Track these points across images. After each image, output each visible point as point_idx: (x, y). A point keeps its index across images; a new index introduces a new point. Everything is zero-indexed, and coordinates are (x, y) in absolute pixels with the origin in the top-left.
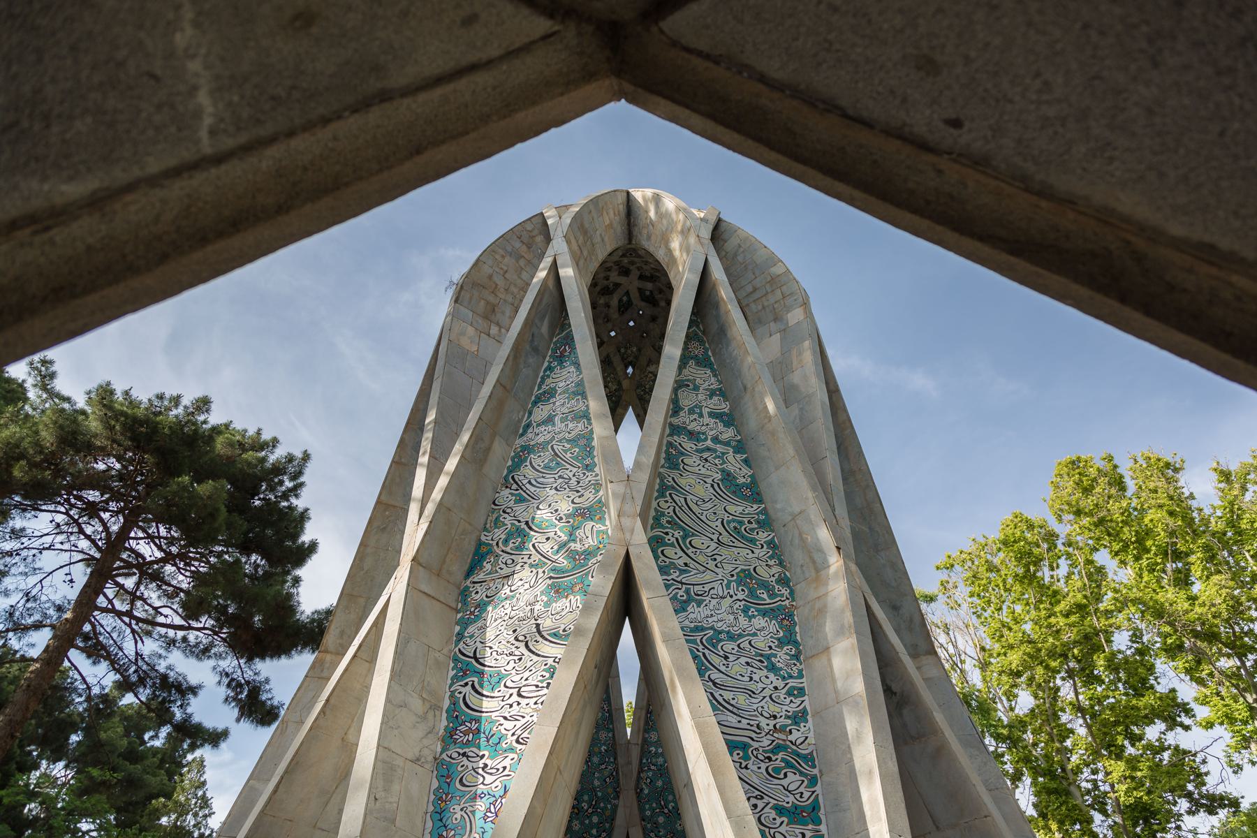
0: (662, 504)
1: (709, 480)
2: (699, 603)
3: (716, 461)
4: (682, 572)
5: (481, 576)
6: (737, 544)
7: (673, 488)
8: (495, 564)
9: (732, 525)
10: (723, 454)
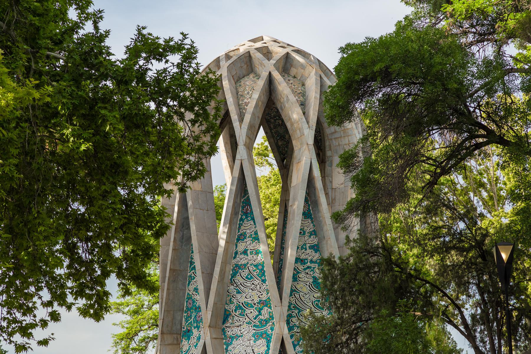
0: (292, 299)
1: (308, 284)
3: (311, 273)
5: (228, 325)
6: (317, 311)
7: (295, 290)
8: (233, 320)
9: (316, 302)
10: (314, 268)
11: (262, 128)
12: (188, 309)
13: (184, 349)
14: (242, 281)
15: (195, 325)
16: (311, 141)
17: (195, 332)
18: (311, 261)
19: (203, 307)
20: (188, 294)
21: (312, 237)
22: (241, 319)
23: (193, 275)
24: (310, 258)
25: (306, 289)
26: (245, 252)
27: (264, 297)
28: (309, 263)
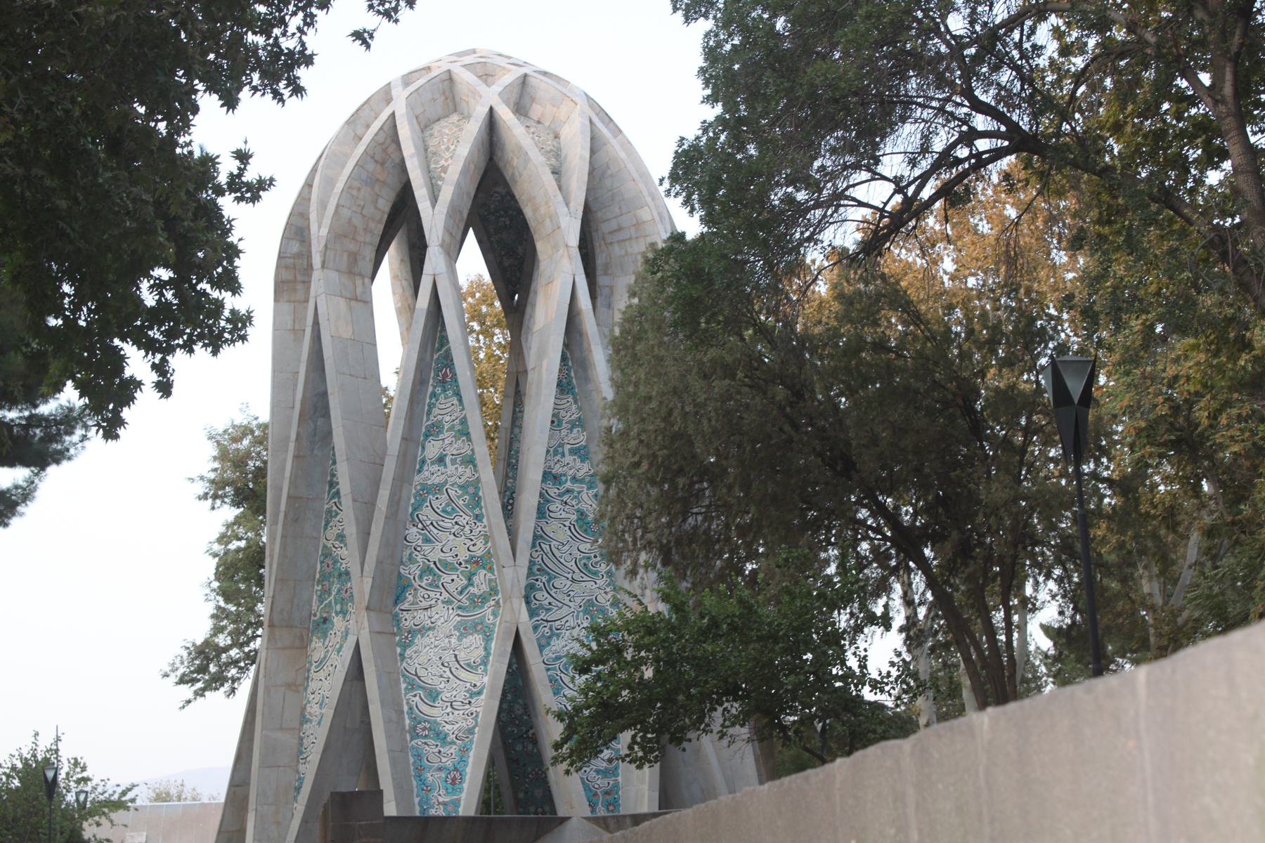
0: (535, 555)
1: (567, 524)
2: (558, 636)
4: (548, 610)
5: (405, 606)
6: (586, 578)
8: (415, 596)
11: (471, 231)
12: (325, 577)
13: (315, 658)
14: (434, 517)
16: (573, 239)
17: (338, 621)
18: (574, 479)
19: (355, 570)
20: (325, 546)
21: (575, 430)
22: (432, 594)
24: (571, 472)
25: (563, 535)
26: (441, 460)
27: (479, 550)
28: (569, 483)
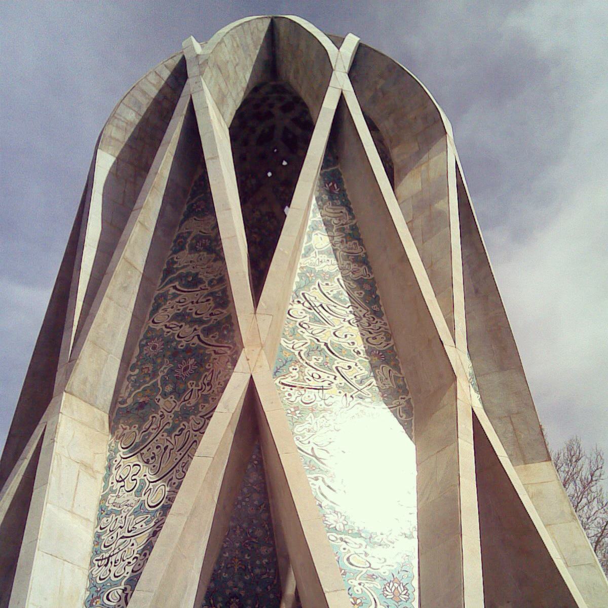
15: (169, 388)
22: (324, 376)
23: (173, 291)
